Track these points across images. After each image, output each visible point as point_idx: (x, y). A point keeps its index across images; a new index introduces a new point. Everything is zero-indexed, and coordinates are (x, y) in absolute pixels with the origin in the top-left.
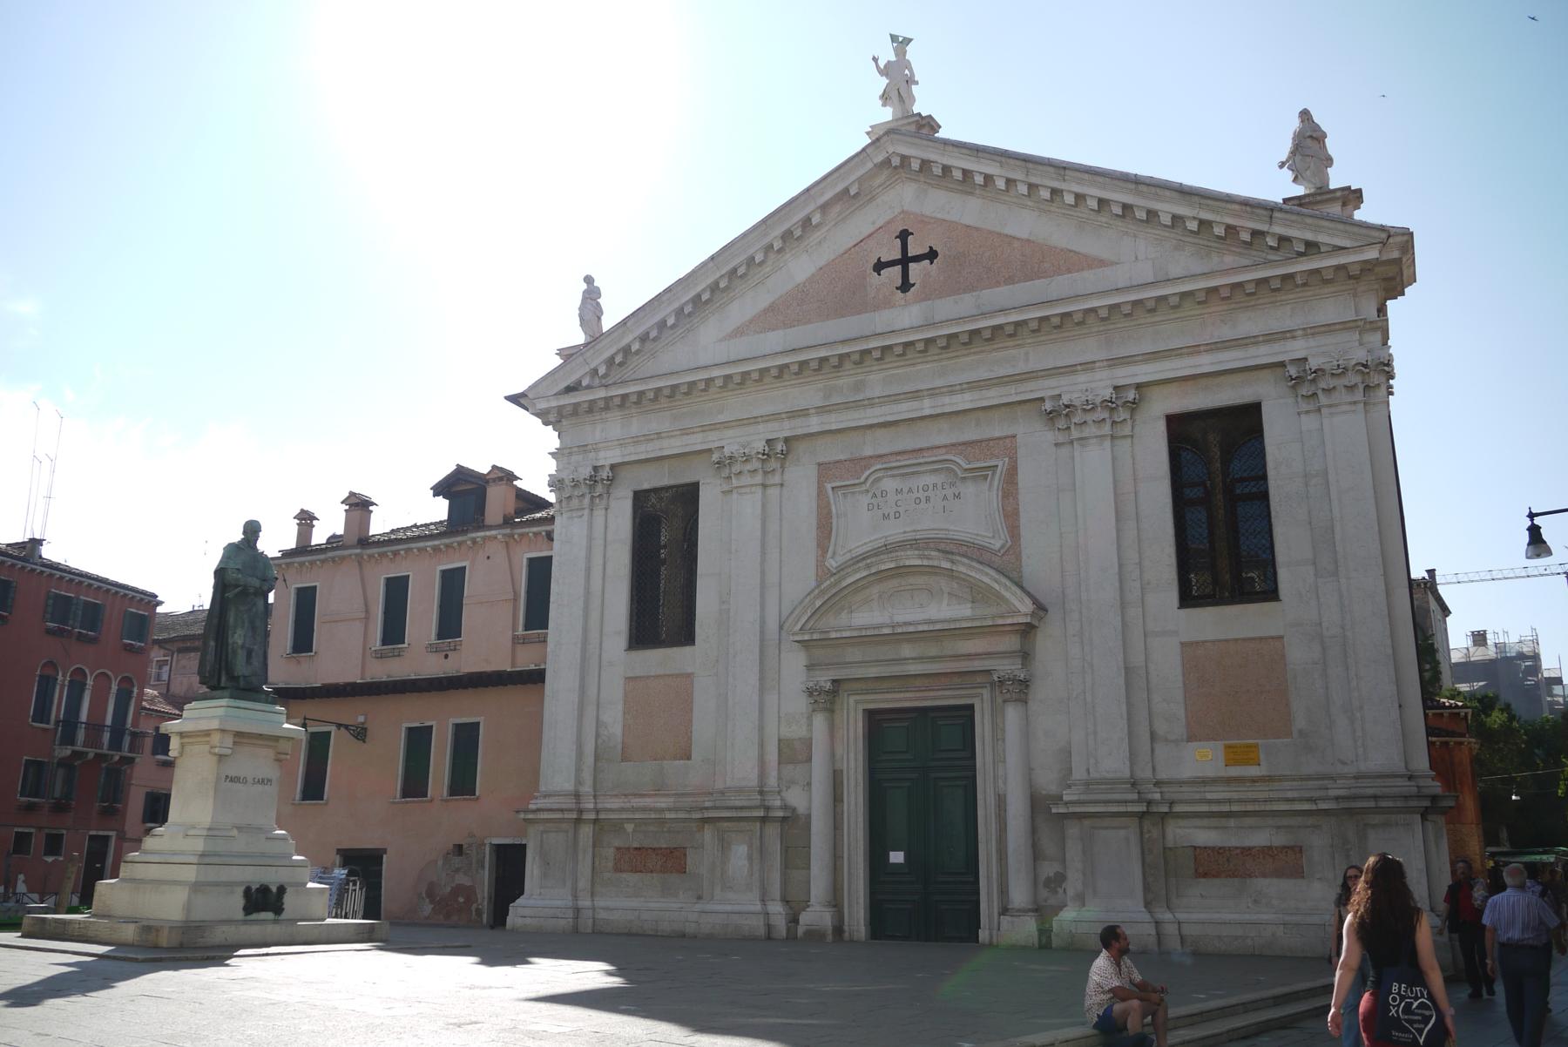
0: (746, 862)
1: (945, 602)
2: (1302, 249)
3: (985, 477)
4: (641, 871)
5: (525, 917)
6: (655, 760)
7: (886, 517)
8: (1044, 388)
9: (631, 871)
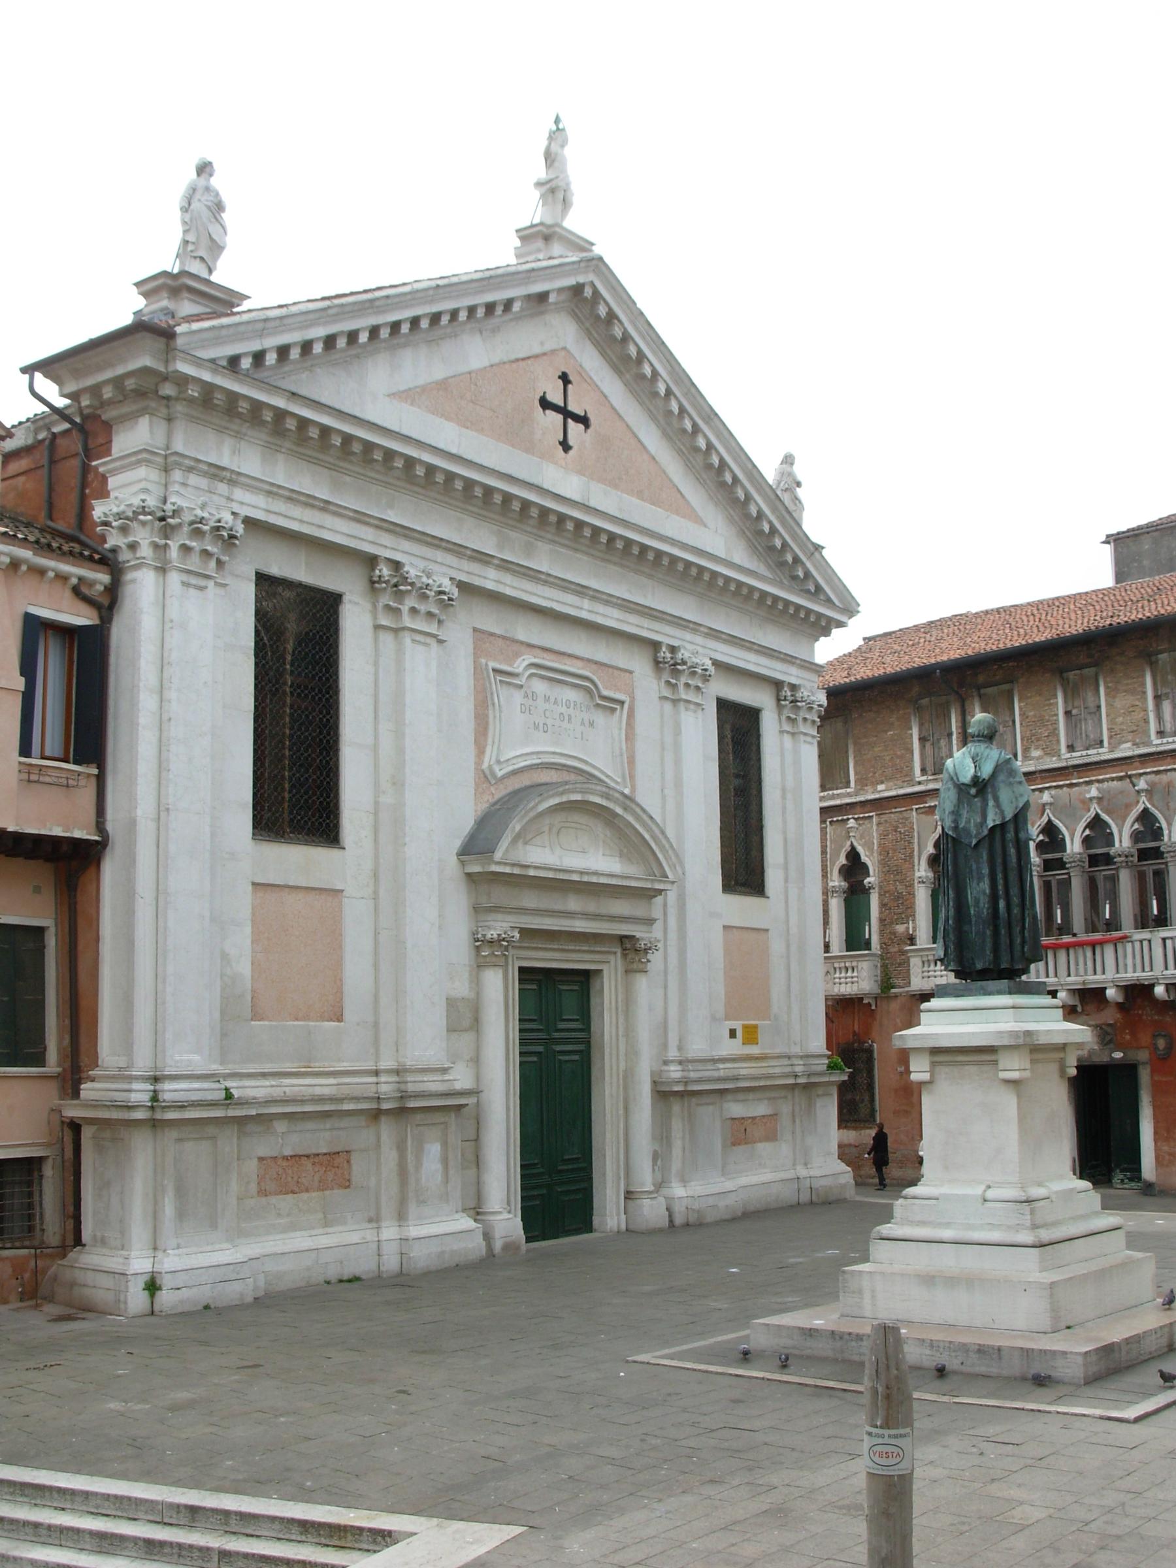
0: (439, 1166)
1: (601, 853)
2: (813, 590)
3: (613, 710)
4: (293, 1192)
5: (178, 1289)
6: (297, 1019)
7: (536, 727)
8: (665, 635)
9: (281, 1193)
